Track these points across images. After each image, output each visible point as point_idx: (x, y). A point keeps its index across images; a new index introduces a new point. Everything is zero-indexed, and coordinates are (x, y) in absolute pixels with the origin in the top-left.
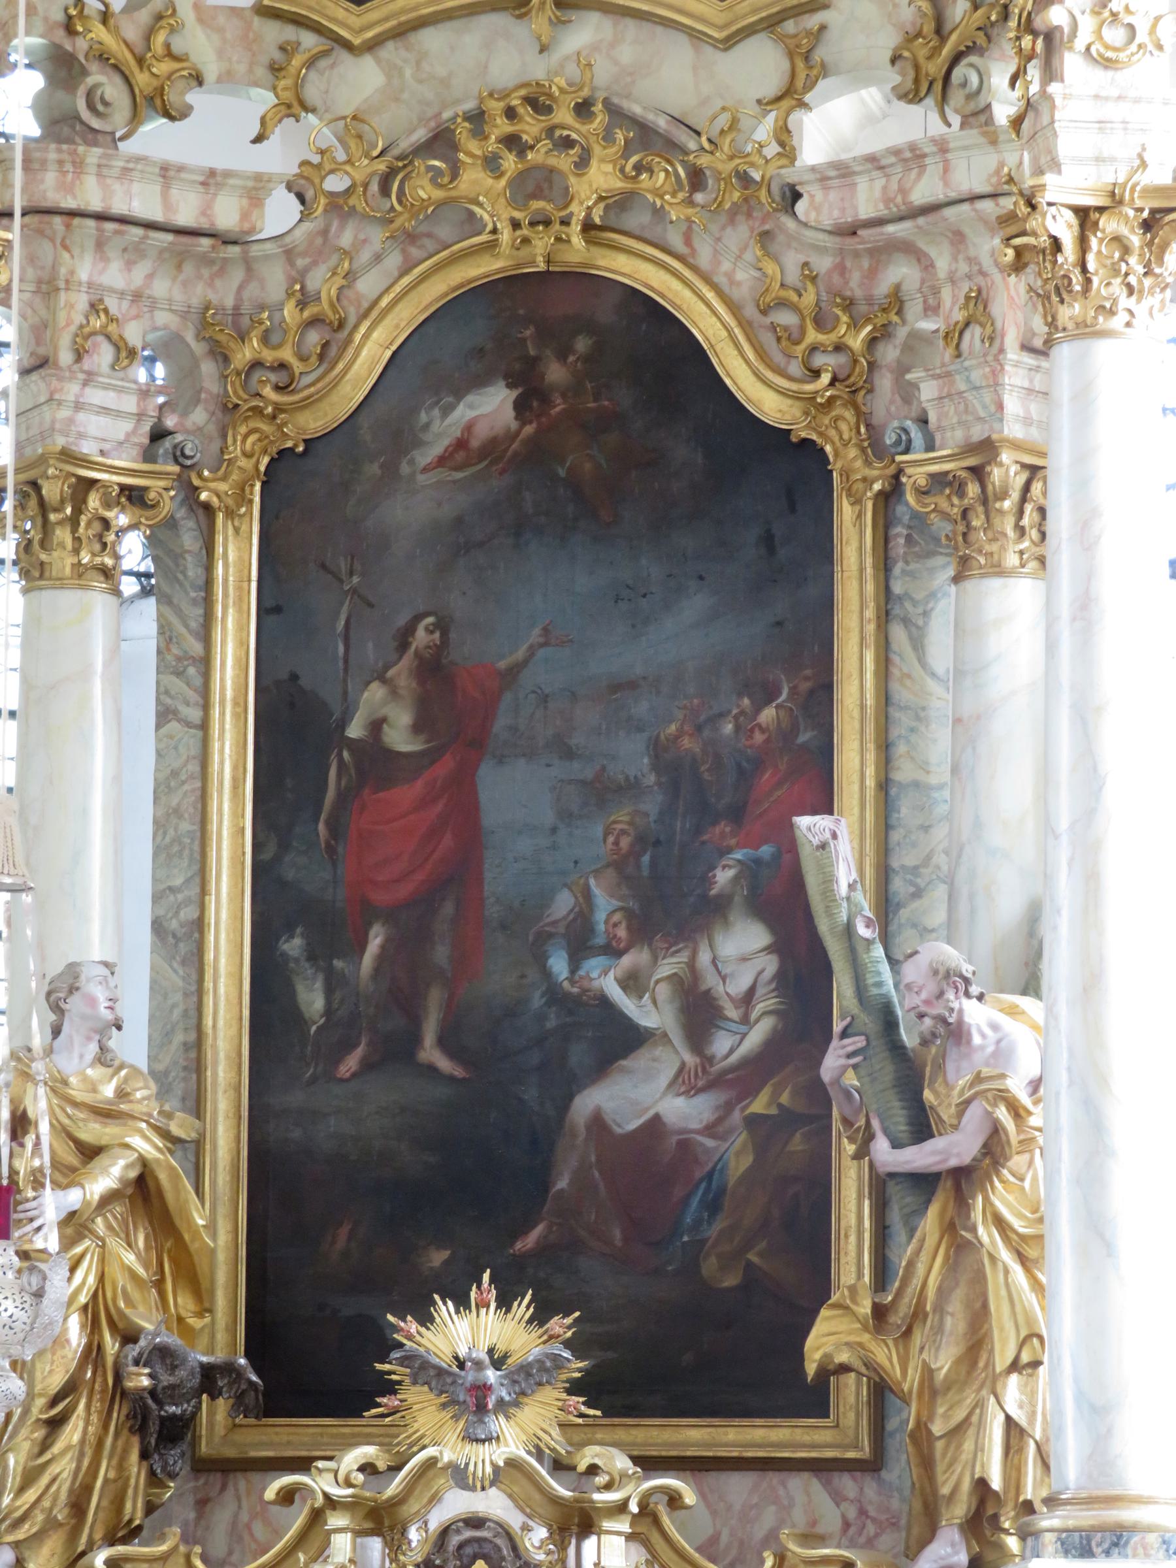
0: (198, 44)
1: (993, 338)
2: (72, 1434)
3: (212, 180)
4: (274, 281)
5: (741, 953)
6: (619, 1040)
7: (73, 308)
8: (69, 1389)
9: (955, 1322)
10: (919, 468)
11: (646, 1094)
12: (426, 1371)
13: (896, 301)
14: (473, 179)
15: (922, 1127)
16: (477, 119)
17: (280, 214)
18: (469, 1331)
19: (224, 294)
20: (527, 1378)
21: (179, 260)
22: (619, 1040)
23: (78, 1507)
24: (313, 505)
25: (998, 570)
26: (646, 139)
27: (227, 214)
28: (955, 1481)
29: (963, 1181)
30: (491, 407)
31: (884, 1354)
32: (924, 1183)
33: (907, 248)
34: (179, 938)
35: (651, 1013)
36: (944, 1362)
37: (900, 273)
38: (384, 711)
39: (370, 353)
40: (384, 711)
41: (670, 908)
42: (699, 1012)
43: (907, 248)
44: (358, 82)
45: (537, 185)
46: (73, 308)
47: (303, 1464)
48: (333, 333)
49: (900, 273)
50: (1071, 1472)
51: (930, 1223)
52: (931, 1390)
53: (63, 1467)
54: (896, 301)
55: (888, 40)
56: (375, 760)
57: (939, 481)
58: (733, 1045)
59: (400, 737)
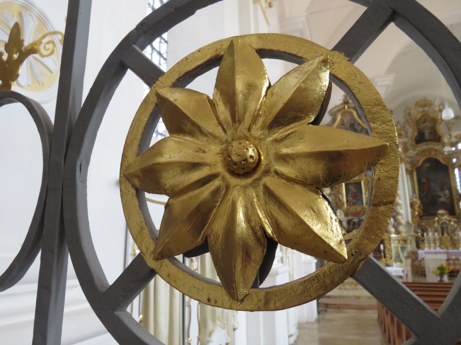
5: (447, 192)
6: (440, 197)
11: (442, 199)
12: (439, 214)
18: (440, 212)
20: (445, 214)
22: (440, 197)
24: (419, 170)
26: (436, 150)
30: (428, 165)
34: (414, 192)
35: (442, 195)
38: (424, 180)
39: (421, 162)
40: (424, 180)
41: (442, 189)
42: (445, 195)
45: (430, 153)
48: (418, 162)
56: (424, 183)
58: (448, 196)
59: (425, 181)
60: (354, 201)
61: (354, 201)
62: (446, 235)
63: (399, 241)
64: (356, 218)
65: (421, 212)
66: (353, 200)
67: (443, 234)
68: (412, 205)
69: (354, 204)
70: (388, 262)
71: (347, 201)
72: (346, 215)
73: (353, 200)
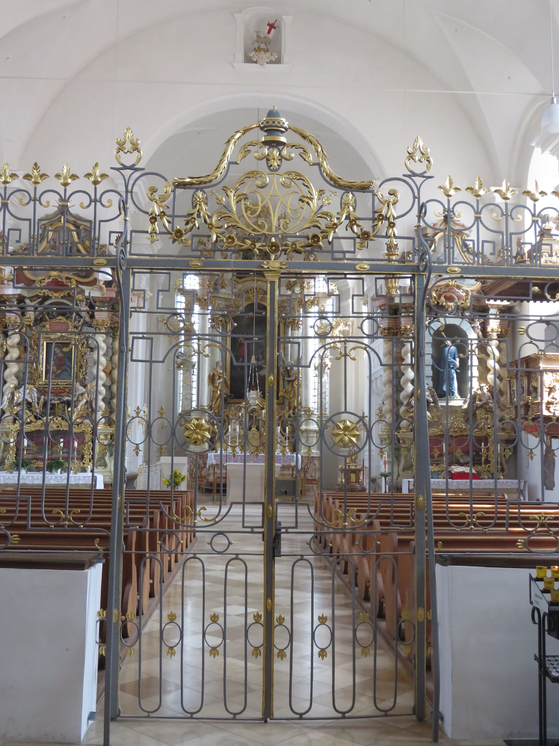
0: (227, 282)
1: (295, 310)
2: (218, 401)
3: (229, 294)
4: (232, 303)
7: (216, 305)
8: (218, 397)
9: (292, 393)
10: (288, 321)
13: (285, 306)
14: (250, 295)
15: (289, 377)
16: (251, 290)
17: (234, 297)
19: (228, 303)
21: (224, 301)
23: (219, 407)
25: (295, 330)
27: (230, 297)
28: (292, 406)
29: (293, 381)
31: (286, 395)
32: (289, 381)
33: (287, 302)
36: (292, 396)
37: (286, 304)
43: (287, 302)
44: (240, 286)
46: (216, 305)
47: (240, 403)
49: (286, 304)
50: (304, 405)
51: (290, 384)
52: (290, 398)
53: (218, 403)
54: (285, 306)
55: (285, 285)
57: (290, 322)
60: (59, 371)
61: (59, 371)
62: (254, 429)
63: (106, 435)
64: (56, 398)
65: (227, 391)
66: (57, 370)
67: (250, 429)
68: (212, 379)
69: (57, 376)
70: (85, 465)
71: (47, 371)
72: (42, 391)
73: (57, 370)
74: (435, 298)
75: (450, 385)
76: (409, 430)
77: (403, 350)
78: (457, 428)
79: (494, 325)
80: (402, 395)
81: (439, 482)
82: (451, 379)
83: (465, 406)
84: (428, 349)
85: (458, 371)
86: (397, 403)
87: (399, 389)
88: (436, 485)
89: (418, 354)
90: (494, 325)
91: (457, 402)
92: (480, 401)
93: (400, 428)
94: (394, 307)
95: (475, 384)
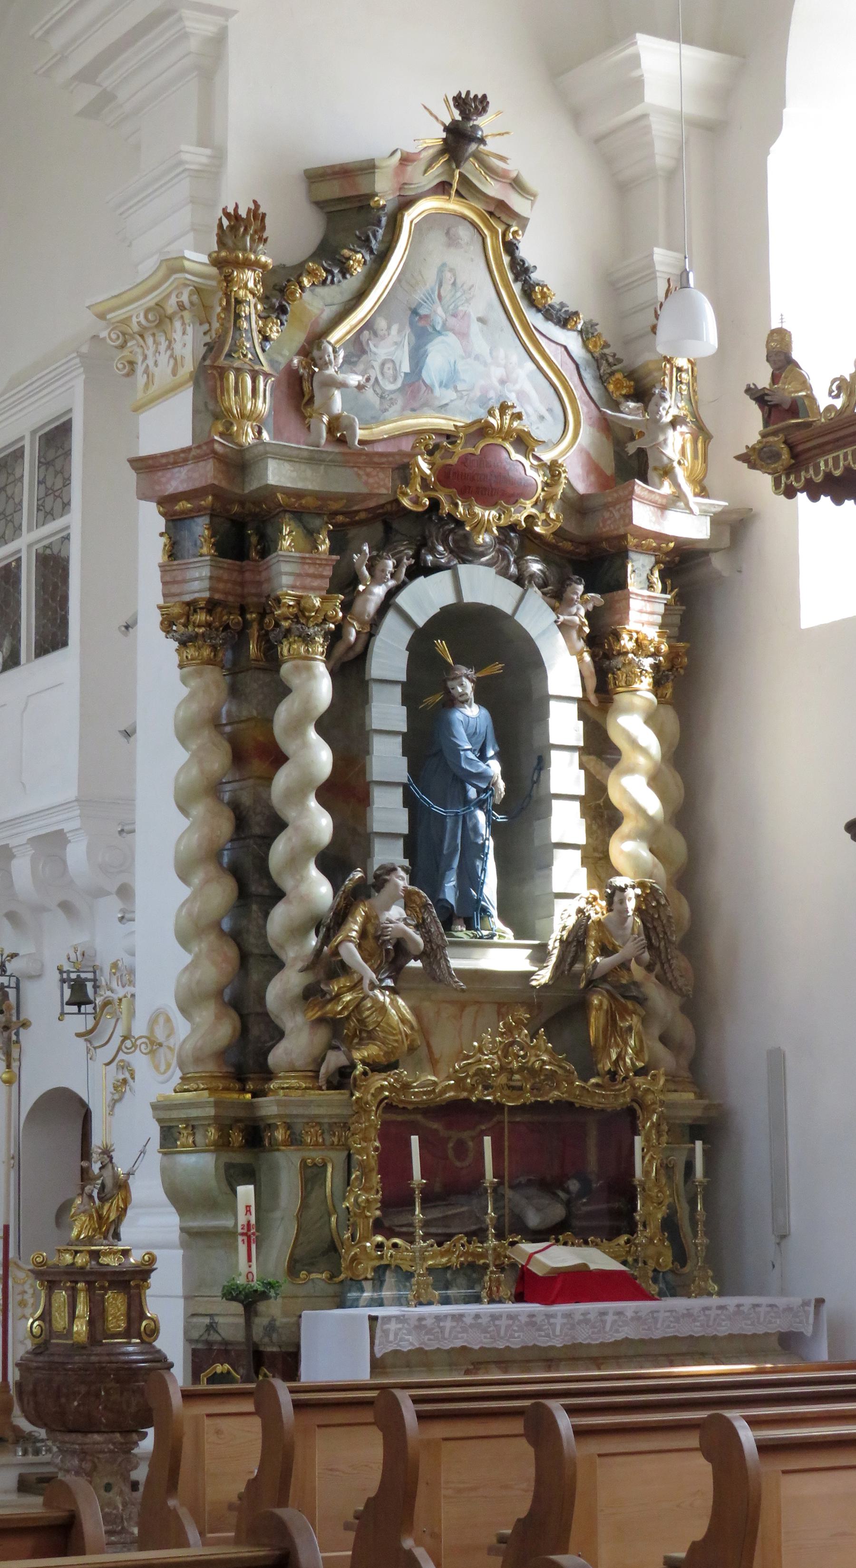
74: (425, 483)
75: (470, 880)
76: (322, 1081)
77: (283, 713)
78: (521, 1069)
79: (644, 614)
80: (280, 918)
81: (494, 1317)
82: (472, 851)
83: (544, 976)
84: (388, 712)
85: (500, 818)
86: (244, 958)
87: (255, 888)
88: (429, 1331)
89: (344, 725)
90: (644, 614)
91: (504, 956)
92: (605, 950)
93: (268, 1074)
94: (236, 508)
95: (568, 873)
